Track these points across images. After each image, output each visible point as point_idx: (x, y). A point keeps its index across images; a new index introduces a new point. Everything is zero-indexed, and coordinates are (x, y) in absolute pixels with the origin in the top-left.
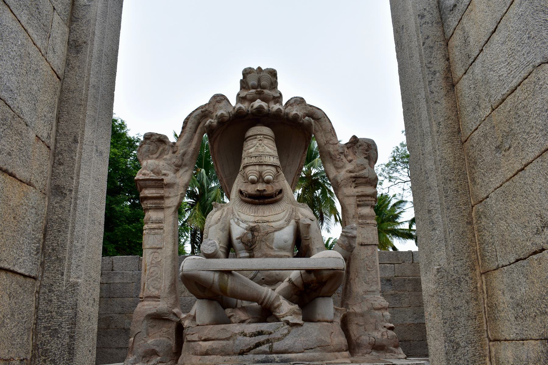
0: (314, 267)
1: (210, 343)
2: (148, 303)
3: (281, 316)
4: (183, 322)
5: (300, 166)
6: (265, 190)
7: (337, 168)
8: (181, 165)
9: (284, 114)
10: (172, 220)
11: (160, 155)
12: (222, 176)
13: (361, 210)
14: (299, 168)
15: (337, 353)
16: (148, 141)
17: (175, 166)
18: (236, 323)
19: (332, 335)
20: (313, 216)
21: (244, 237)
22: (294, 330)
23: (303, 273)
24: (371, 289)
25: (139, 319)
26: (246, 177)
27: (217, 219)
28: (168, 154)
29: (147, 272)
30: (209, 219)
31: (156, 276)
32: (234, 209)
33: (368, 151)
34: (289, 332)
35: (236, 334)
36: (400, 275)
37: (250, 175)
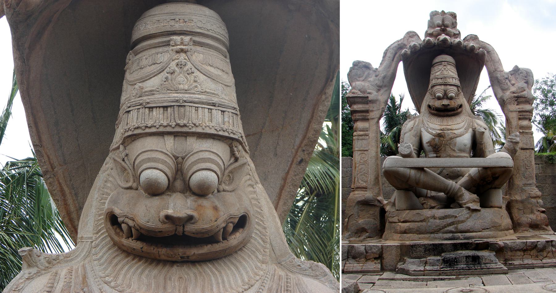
2: (358, 192)
6: (449, 105)
18: (427, 208)
20: (485, 126)
21: (432, 142)
26: (433, 95)
29: (357, 169)
32: (424, 120)
34: (471, 216)
35: (428, 217)
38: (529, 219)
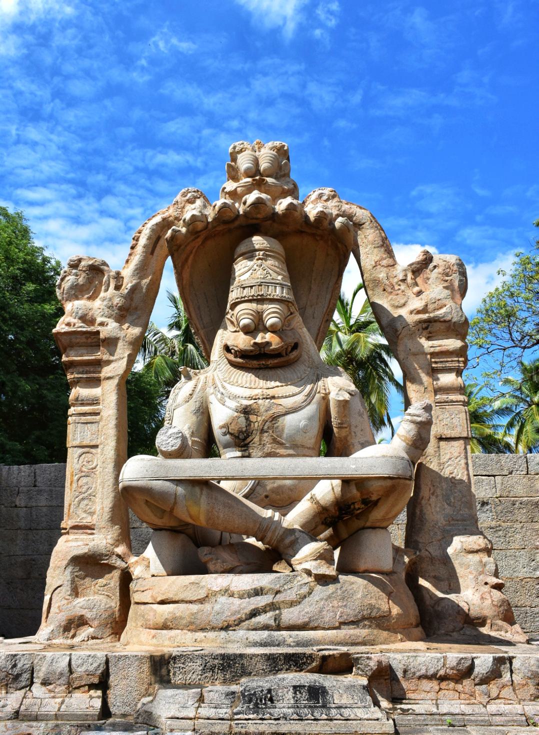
0: (357, 473)
3: (297, 562)
4: (131, 569)
5: (330, 306)
6: (268, 344)
12: (198, 326)
14: (329, 310)
16: (74, 271)
17: (118, 309)
18: (216, 572)
23: (336, 485)
25: (60, 563)
27: (188, 395)
29: (74, 485)
31: (88, 493)
32: (216, 378)
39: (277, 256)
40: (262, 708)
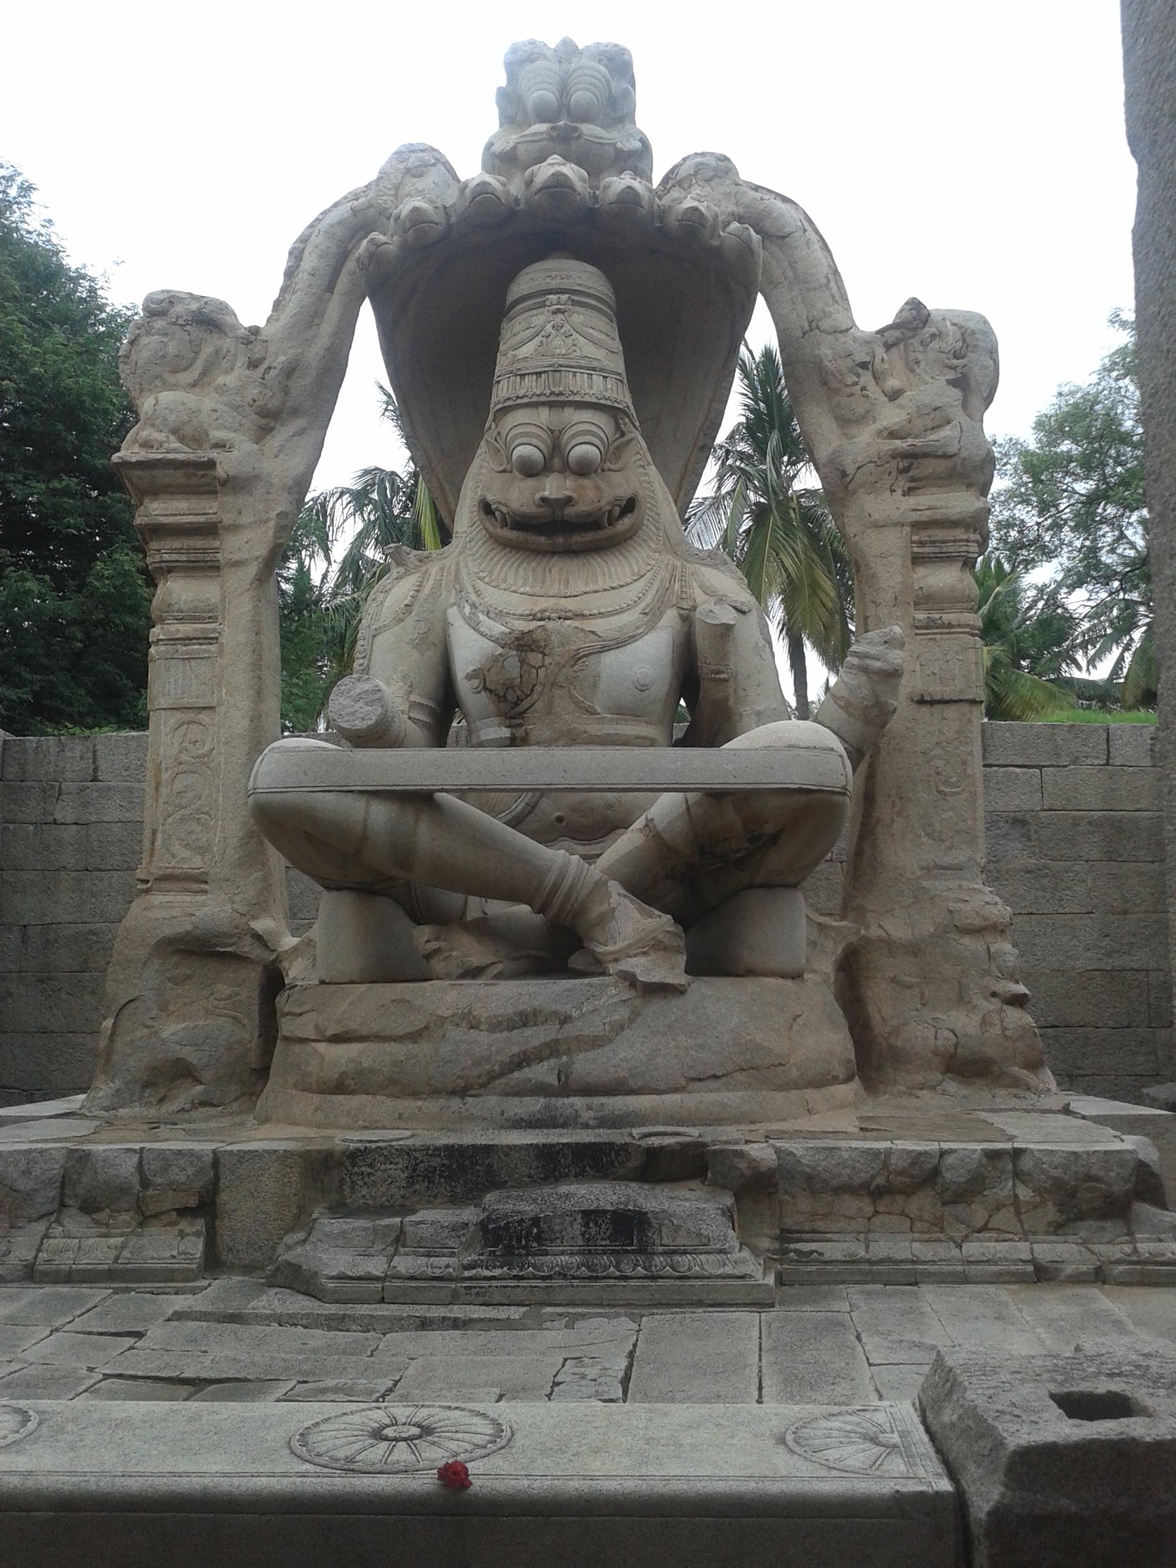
1: (354, 1049)
2: (167, 899)
3: (611, 957)
4: (285, 964)
6: (569, 501)
7: (846, 422)
8: (281, 411)
9: (651, 212)
10: (249, 607)
11: (205, 373)
13: (924, 577)
15: (809, 1091)
16: (159, 324)
18: (448, 976)
19: (795, 1027)
21: (493, 672)
22: (656, 1006)
24: (947, 860)
28: (232, 369)
29: (164, 791)
30: (374, 605)
32: (463, 571)
33: (964, 357)
34: (636, 1014)
35: (443, 1020)
36: (1058, 805)
37: (516, 443)
38: (946, 1033)
39: (600, 305)
40: (520, 1255)
